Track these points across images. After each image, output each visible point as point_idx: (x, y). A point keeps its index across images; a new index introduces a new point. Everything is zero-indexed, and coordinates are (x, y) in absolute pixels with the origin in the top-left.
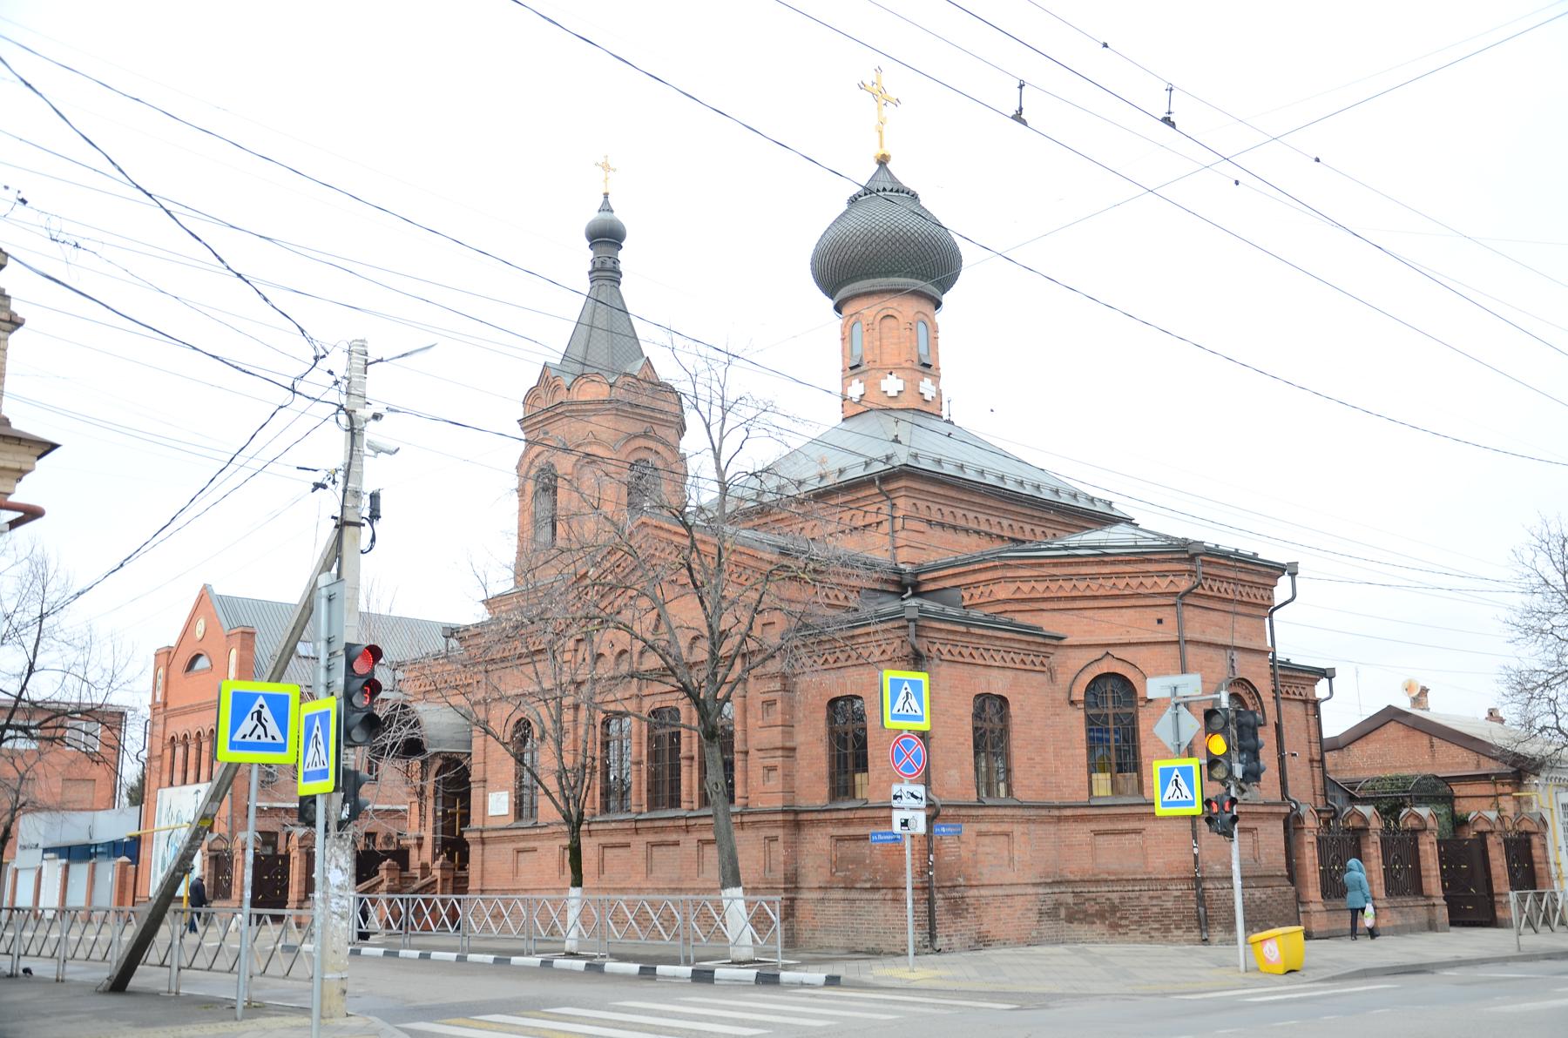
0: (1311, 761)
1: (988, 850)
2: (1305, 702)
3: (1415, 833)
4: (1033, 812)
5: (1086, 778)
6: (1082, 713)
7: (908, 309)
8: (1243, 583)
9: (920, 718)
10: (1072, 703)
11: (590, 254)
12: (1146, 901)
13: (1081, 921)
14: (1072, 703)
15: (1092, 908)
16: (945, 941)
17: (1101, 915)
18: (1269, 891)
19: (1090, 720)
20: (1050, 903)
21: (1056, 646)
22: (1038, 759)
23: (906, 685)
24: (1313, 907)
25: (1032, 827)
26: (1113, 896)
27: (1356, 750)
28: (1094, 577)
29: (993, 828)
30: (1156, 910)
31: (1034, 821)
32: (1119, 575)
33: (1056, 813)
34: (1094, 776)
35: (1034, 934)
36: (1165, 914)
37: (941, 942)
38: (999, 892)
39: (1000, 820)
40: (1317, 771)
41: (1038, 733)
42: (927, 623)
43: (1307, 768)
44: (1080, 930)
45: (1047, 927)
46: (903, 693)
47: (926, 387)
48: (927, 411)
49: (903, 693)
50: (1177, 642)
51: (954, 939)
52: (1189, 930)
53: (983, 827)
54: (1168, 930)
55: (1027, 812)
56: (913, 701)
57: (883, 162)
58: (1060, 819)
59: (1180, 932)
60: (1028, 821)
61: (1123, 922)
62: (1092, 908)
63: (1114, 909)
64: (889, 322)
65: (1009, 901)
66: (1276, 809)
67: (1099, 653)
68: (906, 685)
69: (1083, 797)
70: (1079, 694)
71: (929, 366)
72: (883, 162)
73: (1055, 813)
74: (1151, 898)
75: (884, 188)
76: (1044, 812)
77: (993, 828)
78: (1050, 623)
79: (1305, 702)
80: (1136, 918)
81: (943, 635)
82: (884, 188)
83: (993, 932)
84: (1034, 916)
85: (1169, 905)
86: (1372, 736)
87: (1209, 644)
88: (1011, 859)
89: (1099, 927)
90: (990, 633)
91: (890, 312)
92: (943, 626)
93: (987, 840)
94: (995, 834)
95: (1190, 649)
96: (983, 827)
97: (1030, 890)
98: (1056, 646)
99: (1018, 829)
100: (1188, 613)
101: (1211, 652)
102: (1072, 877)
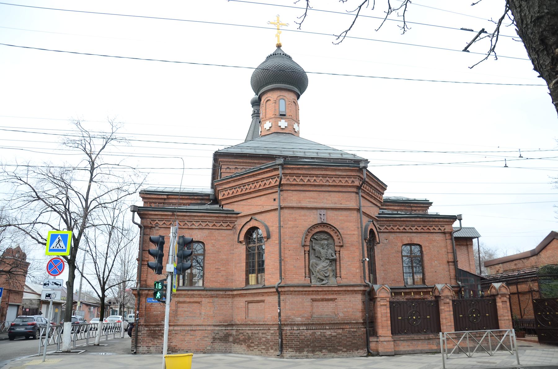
0: (448, 262)
1: (186, 309)
2: (444, 233)
3: (493, 298)
4: (213, 293)
5: (244, 277)
6: (244, 247)
7: (291, 96)
8: (331, 176)
9: (65, 250)
10: (241, 242)
11: (252, 109)
12: (260, 335)
13: (238, 343)
14: (241, 242)
15: (241, 337)
16: (146, 349)
17: (244, 341)
18: (340, 331)
19: (248, 250)
20: (221, 334)
21: (237, 217)
22: (222, 269)
23: (59, 236)
24: (381, 339)
25: (216, 299)
26: (249, 332)
27: (543, 254)
28: (248, 184)
29: (188, 300)
30: (264, 339)
31: (217, 297)
32: (257, 181)
33: (230, 293)
34: (250, 275)
35: (209, 348)
36: (267, 341)
37: (140, 349)
38: (187, 328)
39: (193, 296)
40: (452, 267)
41: (224, 257)
42: (146, 212)
43: (446, 266)
44: (236, 347)
45: (217, 345)
46: (57, 240)
47: (283, 123)
48: (294, 133)
49: (57, 240)
50: (282, 208)
51: (151, 348)
52: (276, 350)
53: (181, 299)
54: (268, 350)
55: (209, 293)
56: (62, 244)
57: (279, 46)
58: (234, 296)
59: (272, 351)
60: (212, 297)
61: (252, 345)
62: (241, 337)
63: (249, 338)
64: (269, 102)
65: (192, 333)
66: (356, 289)
67: (248, 219)
68: (59, 236)
69: (243, 285)
70: (242, 238)
71: (285, 115)
72: (279, 46)
73: (227, 293)
74: (263, 333)
75: (279, 53)
76: (221, 293)
77: (188, 300)
78: (236, 207)
79: (444, 233)
80: (257, 343)
81: (159, 217)
82: (279, 53)
83: (179, 346)
84: (209, 340)
85: (269, 337)
86: (548, 247)
87: (302, 208)
88: (201, 314)
89: (244, 347)
90: (188, 214)
91: (268, 99)
92: (156, 213)
93: (185, 305)
94: (190, 302)
95: (286, 211)
96: (181, 299)
97: (209, 328)
98: (237, 217)
99: (205, 301)
100: (285, 194)
101: (303, 212)
102: (238, 323)
